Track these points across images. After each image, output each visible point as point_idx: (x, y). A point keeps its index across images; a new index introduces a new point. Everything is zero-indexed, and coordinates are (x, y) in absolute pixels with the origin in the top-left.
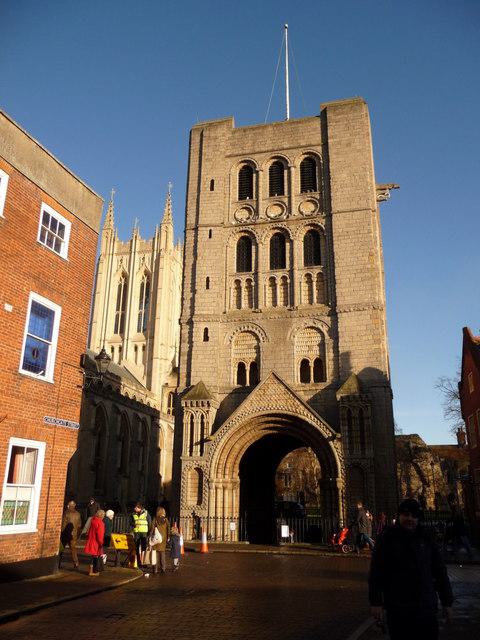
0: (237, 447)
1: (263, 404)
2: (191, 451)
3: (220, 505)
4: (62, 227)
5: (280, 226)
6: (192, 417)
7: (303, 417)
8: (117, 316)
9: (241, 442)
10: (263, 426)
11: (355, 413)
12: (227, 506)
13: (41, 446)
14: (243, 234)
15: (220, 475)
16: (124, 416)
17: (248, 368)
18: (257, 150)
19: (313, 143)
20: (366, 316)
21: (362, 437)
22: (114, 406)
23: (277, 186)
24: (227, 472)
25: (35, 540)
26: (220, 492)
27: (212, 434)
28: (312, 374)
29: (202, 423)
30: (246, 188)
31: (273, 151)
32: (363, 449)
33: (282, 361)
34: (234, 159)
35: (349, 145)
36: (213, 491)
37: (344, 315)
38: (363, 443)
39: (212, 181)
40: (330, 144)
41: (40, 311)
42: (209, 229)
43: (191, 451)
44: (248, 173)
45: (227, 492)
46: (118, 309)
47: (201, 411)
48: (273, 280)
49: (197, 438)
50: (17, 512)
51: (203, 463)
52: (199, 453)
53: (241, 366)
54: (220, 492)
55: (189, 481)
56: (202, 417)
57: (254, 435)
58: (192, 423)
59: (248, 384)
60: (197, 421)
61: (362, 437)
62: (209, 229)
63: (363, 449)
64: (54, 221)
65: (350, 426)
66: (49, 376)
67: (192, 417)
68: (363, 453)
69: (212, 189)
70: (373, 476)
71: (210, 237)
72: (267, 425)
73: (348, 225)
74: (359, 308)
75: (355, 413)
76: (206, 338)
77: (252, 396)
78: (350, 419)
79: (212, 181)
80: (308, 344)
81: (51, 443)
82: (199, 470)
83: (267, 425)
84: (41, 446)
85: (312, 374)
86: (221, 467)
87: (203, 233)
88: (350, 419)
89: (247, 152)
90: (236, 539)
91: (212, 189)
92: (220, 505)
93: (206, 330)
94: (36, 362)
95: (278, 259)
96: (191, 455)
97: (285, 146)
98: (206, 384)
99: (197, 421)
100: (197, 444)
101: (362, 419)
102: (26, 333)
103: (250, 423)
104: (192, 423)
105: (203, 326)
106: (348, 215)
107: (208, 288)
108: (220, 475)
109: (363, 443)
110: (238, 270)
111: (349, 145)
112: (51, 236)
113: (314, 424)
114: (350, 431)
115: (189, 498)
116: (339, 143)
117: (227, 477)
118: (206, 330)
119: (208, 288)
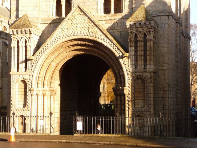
0: (54, 64)
1: (71, 31)
2: (18, 68)
3: (40, 107)
6: (18, 42)
9: (57, 61)
10: (73, 48)
21: (145, 56)
26: (41, 98)
27: (33, 55)
29: (26, 47)
32: (145, 65)
36: (34, 97)
38: (145, 60)
43: (18, 68)
45: (45, 97)
47: (25, 37)
49: (22, 58)
51: (26, 77)
52: (24, 69)
54: (41, 98)
57: (67, 55)
58: (18, 47)
59: (63, 16)
60: (22, 45)
61: (145, 56)
63: (145, 65)
65: (136, 47)
67: (18, 42)
68: (145, 68)
70: (152, 84)
72: (76, 48)
75: (140, 37)
77: (63, 25)
78: (136, 42)
82: (24, 82)
83: (76, 48)
86: (40, 79)
88: (136, 42)
90: (57, 133)
92: (40, 107)
96: (18, 71)
98: (30, 16)
99: (22, 45)
100: (22, 62)
101: (145, 41)
103: (61, 46)
104: (18, 47)
108: (39, 85)
113: (109, 46)
114: (136, 51)
115: (17, 102)
117: (45, 86)
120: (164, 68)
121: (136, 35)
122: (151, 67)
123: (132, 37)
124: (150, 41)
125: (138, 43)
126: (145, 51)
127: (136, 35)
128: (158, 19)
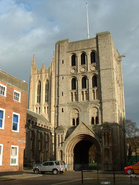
0: (73, 144)
1: (80, 131)
2: (59, 146)
3: (68, 161)
4: (19, 94)
5: (84, 74)
6: (59, 136)
7: (91, 135)
8: (38, 96)
9: (74, 143)
10: (80, 138)
11: (106, 134)
12: (70, 161)
13: (17, 147)
14: (73, 77)
15: (67, 152)
16: (41, 133)
17: (76, 120)
18: (77, 49)
19: (94, 47)
20: (110, 103)
22: (37, 130)
23: (83, 62)
24: (70, 151)
25: (18, 167)
26: (68, 157)
27: (65, 141)
28: (95, 121)
29: (62, 137)
30: (74, 63)
31: (81, 50)
32: (108, 144)
33: (86, 118)
34: (69, 53)
35: (105, 47)
36: (65, 157)
37: (104, 103)
38: (108, 142)
39: (63, 60)
40: (99, 47)
41: (15, 116)
42: (62, 76)
43: (59, 146)
44: (74, 57)
45: (70, 157)
46: (38, 94)
47: (61, 134)
48: (83, 92)
49: (60, 142)
50: (14, 161)
51: (62, 149)
53: (74, 120)
54: (68, 157)
55: (59, 154)
56: (62, 136)
57: (77, 141)
58: (59, 138)
59: (76, 125)
60: (60, 137)
62: (62, 76)
63: (108, 144)
64: (17, 93)
65: (105, 137)
66: (18, 131)
67: (59, 136)
68: (108, 145)
69: (63, 63)
70: (111, 152)
71: (63, 79)
72: (81, 138)
73: (105, 74)
74: (108, 101)
75: (106, 134)
76: (63, 111)
77: (76, 129)
79: (63, 60)
80: (94, 112)
81: (20, 146)
82: (61, 151)
83: (81, 138)
84: (17, 147)
85: (95, 121)
86: (68, 150)
87: (61, 78)
88: (105, 135)
89: (74, 50)
91: (63, 63)
92: (68, 161)
93: (63, 109)
94: (15, 128)
95: (84, 86)
96: (59, 147)
97: (85, 48)
98: (63, 125)
99: (60, 137)
100: (60, 144)
102: (13, 122)
103: (76, 137)
104: (59, 138)
105: (62, 108)
106: (105, 71)
107: (63, 95)
108: (67, 152)
109: (108, 142)
110: (72, 89)
111: (105, 47)
112: (16, 97)
115: (59, 159)
116: (102, 47)
117: (70, 153)
118: (63, 109)
119: (63, 95)
120: (116, 145)
121: (105, 133)
122: (110, 145)
123: (103, 133)
124: (110, 135)
125: (106, 136)
126: (108, 139)
127: (105, 133)
128: (113, 127)
